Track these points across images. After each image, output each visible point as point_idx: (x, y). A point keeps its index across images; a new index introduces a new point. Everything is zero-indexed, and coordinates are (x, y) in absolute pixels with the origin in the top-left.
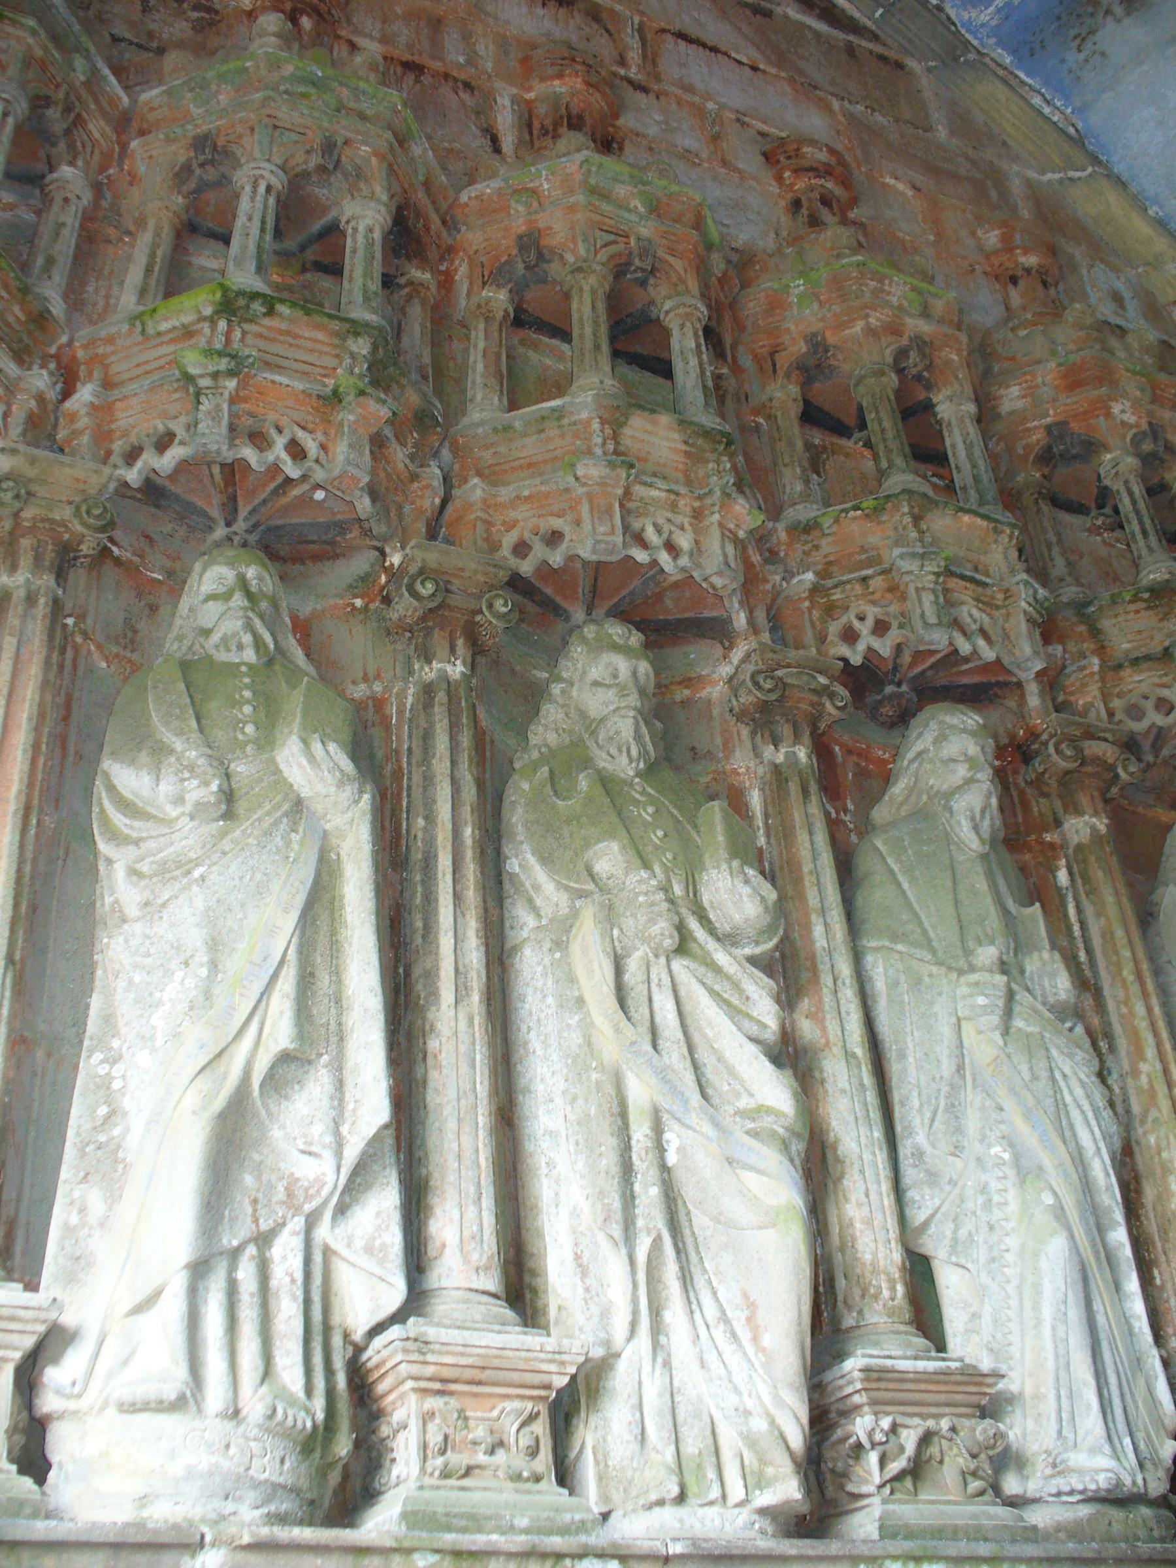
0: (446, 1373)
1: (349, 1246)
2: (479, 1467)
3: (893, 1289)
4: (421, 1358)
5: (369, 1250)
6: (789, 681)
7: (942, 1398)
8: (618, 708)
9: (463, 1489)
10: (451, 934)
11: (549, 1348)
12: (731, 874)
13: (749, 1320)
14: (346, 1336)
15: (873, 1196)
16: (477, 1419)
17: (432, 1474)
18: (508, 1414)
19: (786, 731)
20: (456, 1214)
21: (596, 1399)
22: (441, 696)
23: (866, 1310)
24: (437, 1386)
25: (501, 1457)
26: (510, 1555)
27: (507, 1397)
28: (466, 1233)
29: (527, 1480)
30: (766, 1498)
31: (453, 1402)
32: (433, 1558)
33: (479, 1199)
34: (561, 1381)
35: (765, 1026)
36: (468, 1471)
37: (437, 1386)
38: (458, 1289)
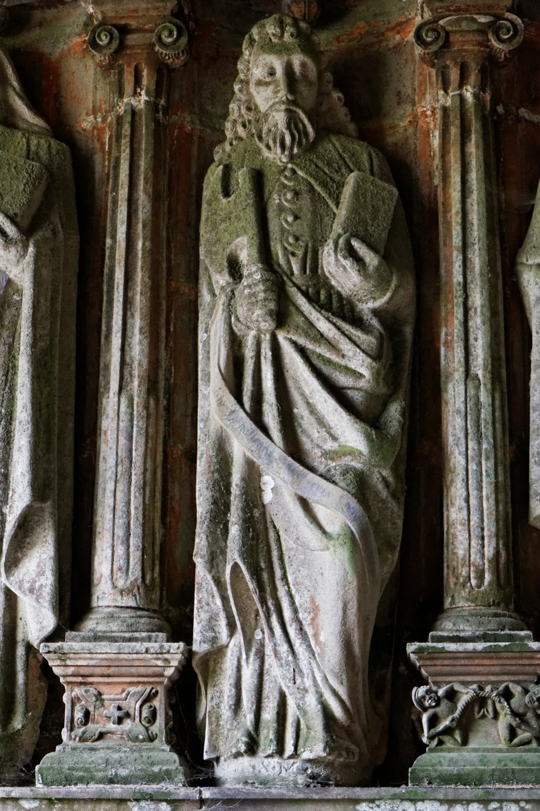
0: (82, 671)
1: (20, 588)
2: (112, 733)
3: (480, 577)
4: (63, 663)
5: (31, 590)
6: (449, 28)
7: (498, 669)
8: (274, 104)
9: (92, 749)
10: (119, 335)
11: (152, 651)
12: (336, 251)
13: (313, 619)
14: (29, 647)
15: (473, 501)
16: (110, 700)
17: (75, 739)
18: (133, 695)
19: (454, 75)
20: (109, 552)
21: (213, 677)
22: (126, 129)
23: (456, 595)
24: (80, 679)
25: (128, 724)
26: (86, 801)
27: (131, 684)
28: (115, 567)
29: (143, 741)
30: (306, 755)
31: (92, 690)
32: (35, 804)
33: (128, 539)
34: (169, 672)
35: (361, 376)
36: (101, 736)
37: (80, 679)
38: (109, 607)
